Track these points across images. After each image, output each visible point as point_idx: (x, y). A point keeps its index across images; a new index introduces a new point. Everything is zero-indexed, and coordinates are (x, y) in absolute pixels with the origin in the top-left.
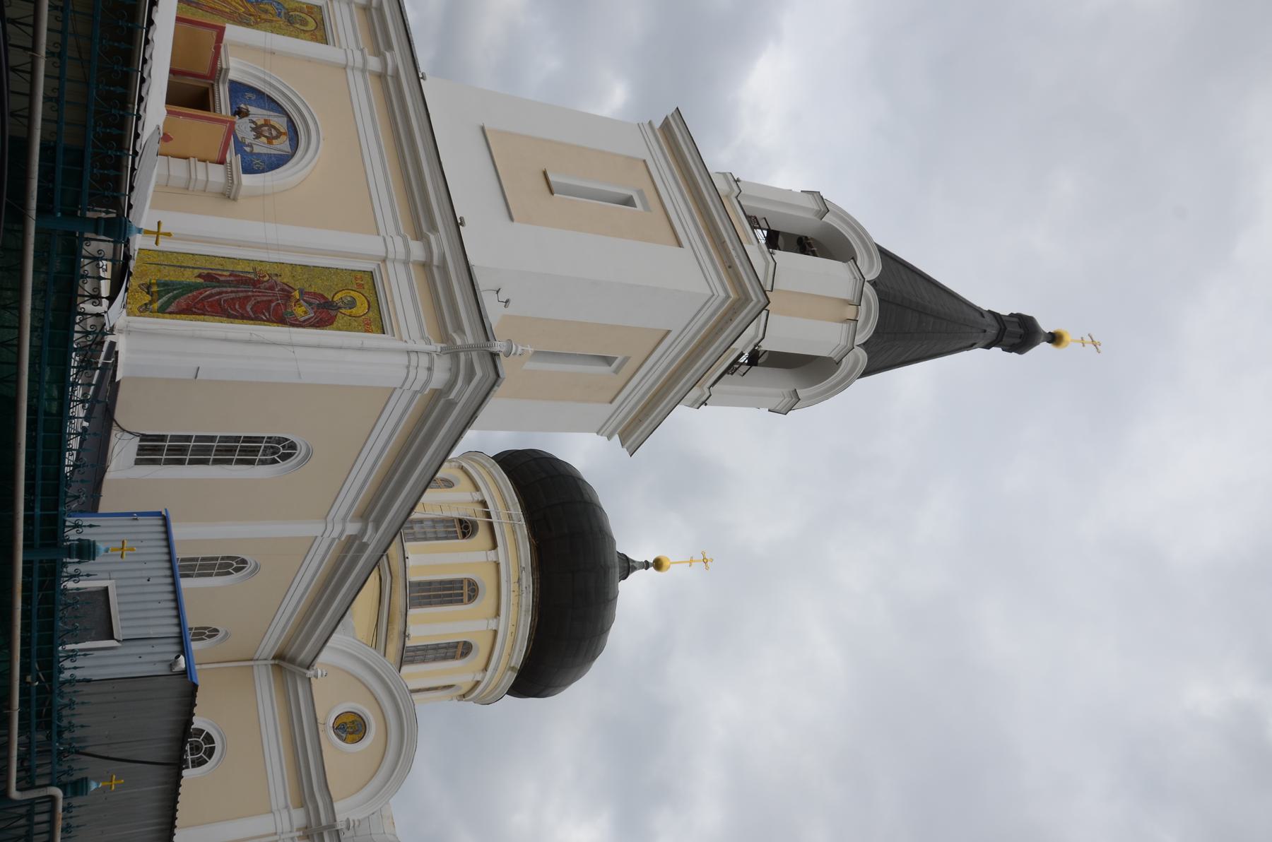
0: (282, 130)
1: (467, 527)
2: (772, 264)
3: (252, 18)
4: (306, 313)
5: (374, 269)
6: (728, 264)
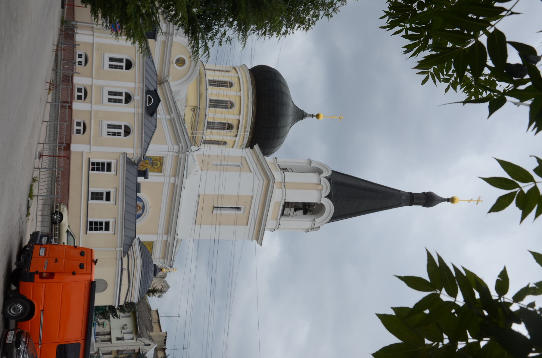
0: (141, 207)
1: (230, 127)
2: (277, 227)
3: (141, 167)
5: (155, 242)
6: (259, 231)
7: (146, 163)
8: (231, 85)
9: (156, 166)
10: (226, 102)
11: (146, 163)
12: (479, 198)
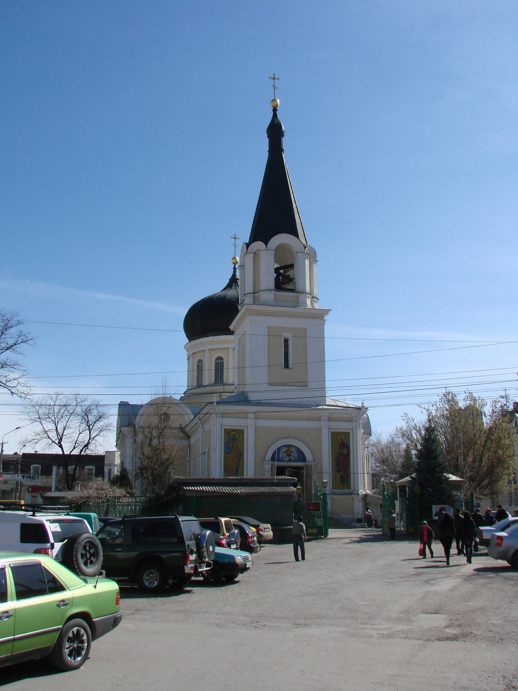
3: (238, 451)
4: (345, 450)
7: (233, 447)
8: (200, 361)
9: (236, 436)
10: (216, 364)
11: (233, 447)
12: (271, 78)
